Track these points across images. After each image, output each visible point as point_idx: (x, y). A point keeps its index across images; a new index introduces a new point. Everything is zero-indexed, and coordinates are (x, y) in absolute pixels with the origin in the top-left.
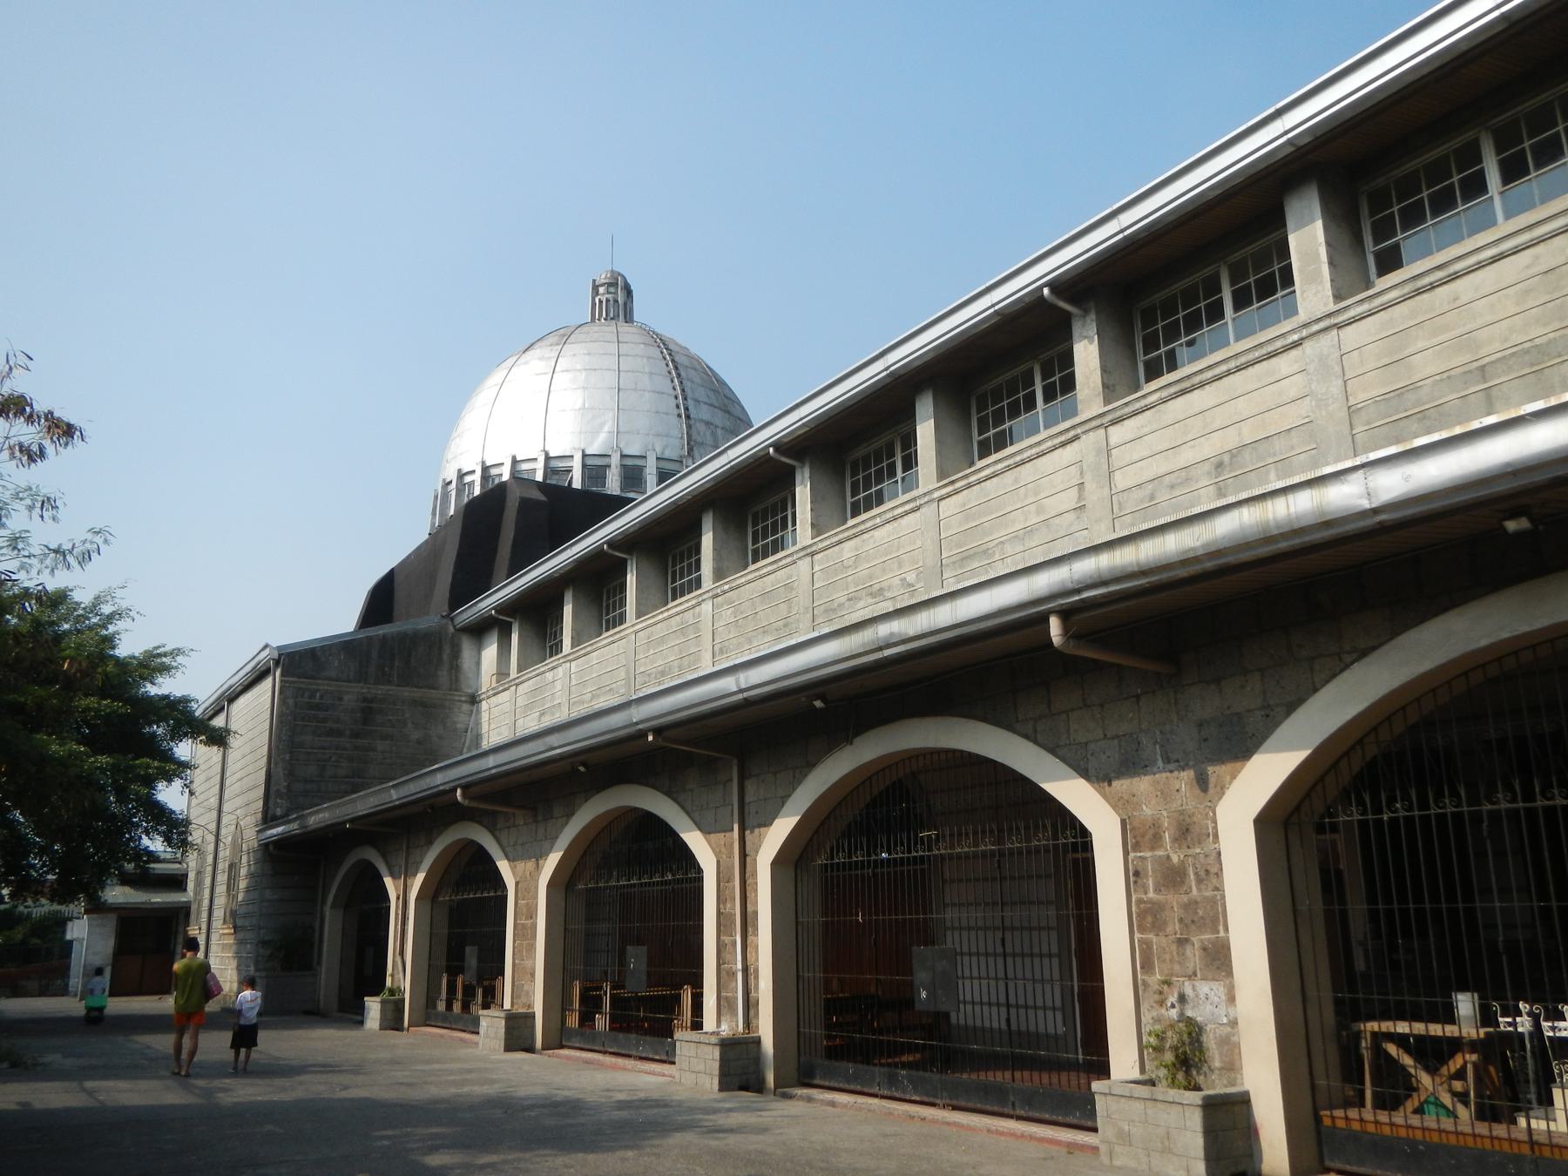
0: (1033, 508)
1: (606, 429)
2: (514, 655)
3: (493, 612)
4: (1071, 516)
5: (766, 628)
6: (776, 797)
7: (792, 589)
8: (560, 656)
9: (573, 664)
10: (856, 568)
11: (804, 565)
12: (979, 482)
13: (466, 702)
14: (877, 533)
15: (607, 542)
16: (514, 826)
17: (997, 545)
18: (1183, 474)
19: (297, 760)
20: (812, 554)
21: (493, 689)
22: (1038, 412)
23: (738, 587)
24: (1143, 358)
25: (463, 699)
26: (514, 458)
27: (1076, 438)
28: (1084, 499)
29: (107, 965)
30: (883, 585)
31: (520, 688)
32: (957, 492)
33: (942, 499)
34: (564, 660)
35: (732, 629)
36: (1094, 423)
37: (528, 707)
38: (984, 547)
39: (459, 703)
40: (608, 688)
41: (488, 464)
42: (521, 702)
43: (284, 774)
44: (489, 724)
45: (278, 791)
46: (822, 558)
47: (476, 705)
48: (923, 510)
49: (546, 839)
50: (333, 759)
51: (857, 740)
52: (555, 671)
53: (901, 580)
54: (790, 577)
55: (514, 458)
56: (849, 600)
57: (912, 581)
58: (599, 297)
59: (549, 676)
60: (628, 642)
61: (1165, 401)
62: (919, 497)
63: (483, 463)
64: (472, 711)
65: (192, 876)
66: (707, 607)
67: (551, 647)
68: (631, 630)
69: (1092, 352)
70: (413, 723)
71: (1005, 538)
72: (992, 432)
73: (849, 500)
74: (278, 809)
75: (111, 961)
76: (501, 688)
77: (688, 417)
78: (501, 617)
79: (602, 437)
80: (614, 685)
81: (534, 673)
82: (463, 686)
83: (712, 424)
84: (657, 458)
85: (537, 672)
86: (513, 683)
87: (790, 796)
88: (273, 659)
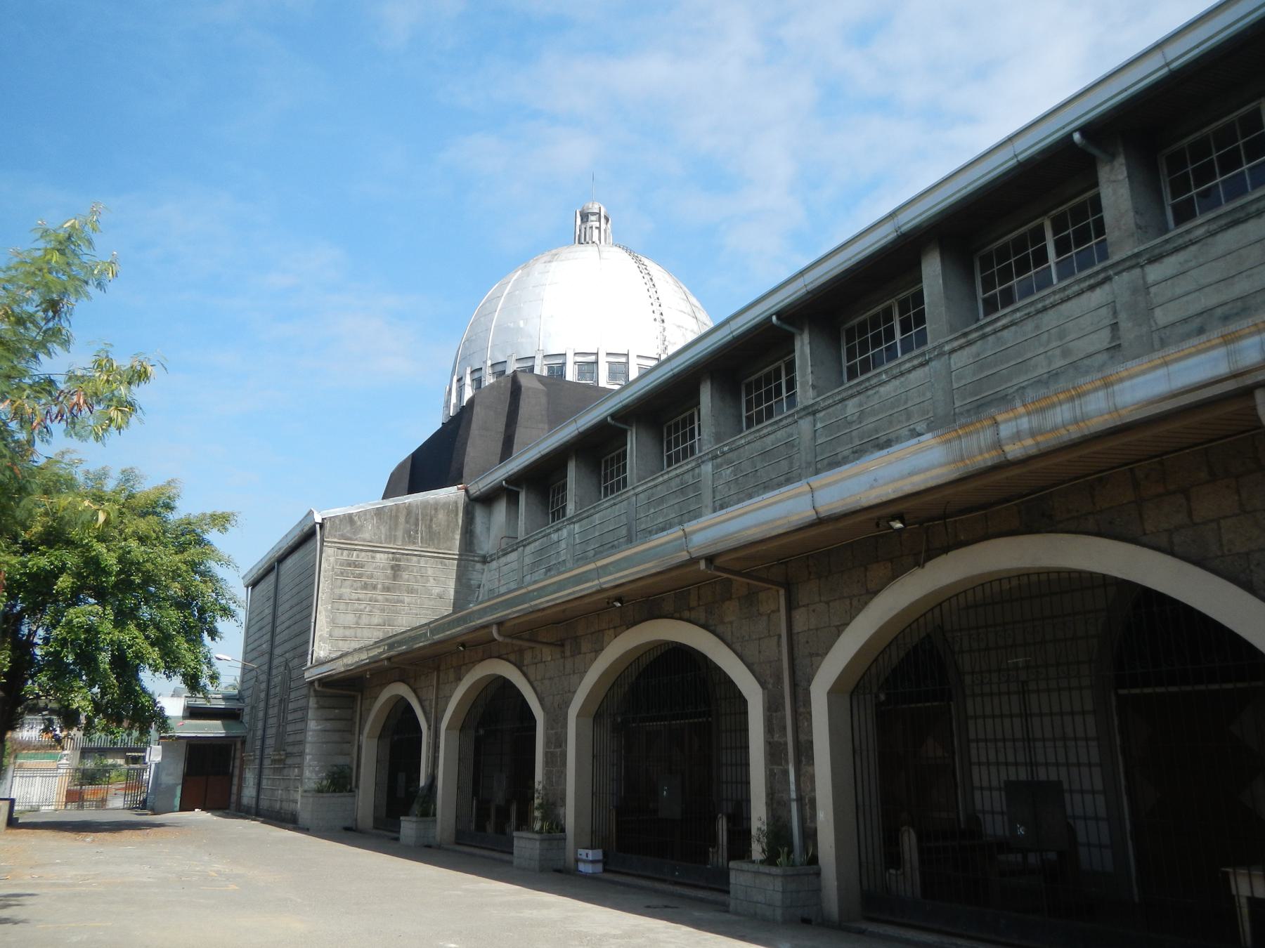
0: (1058, 352)
2: (521, 521)
4: (1105, 356)
5: (766, 484)
6: (830, 626)
7: (793, 446)
8: (565, 519)
9: (577, 526)
10: (860, 422)
11: (805, 425)
12: (995, 332)
13: (478, 562)
14: (882, 389)
16: (542, 662)
17: (1017, 390)
18: (1239, 304)
19: (338, 610)
20: (814, 413)
22: (1050, 266)
23: (739, 448)
24: (1170, 202)
25: (476, 559)
27: (1108, 279)
28: (1119, 338)
29: (177, 785)
30: (890, 436)
32: (970, 344)
33: (953, 351)
35: (732, 486)
36: (1128, 264)
38: (1004, 393)
39: (472, 563)
40: (610, 545)
43: (327, 622)
44: (499, 581)
45: (320, 636)
46: (824, 415)
48: (933, 364)
49: (574, 673)
50: (367, 610)
51: (929, 565)
52: (560, 532)
53: (910, 430)
54: (791, 435)
56: (853, 452)
57: (923, 431)
59: (555, 537)
60: (629, 504)
61: (1213, 234)
62: (929, 352)
64: (484, 570)
65: (247, 710)
66: (707, 468)
67: (553, 514)
68: (632, 492)
69: (1122, 195)
70: (434, 579)
71: (1026, 383)
72: (998, 289)
73: (845, 364)
74: (322, 652)
75: (181, 782)
80: (616, 542)
82: (476, 548)
83: (683, 327)
85: (543, 534)
86: (520, 544)
87: (848, 624)
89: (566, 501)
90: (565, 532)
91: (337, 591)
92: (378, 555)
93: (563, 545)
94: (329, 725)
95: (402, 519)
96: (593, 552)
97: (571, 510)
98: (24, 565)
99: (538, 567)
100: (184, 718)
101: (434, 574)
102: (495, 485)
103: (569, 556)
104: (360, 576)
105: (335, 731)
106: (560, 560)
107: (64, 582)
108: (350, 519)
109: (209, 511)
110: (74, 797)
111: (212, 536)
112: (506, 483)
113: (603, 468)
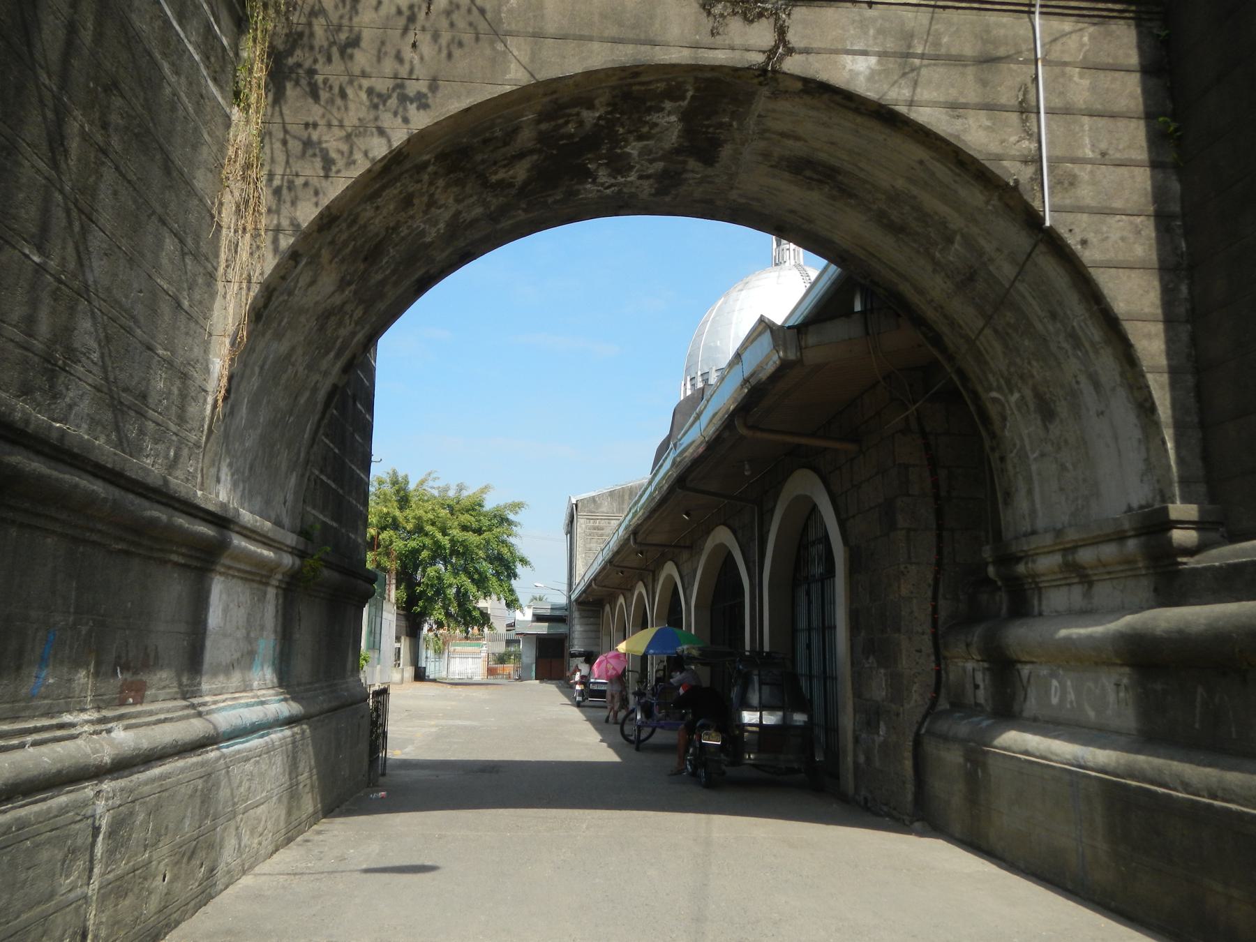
91: (588, 546)
92: (612, 522)
94: (587, 628)
95: (627, 497)
98: (406, 546)
100: (533, 621)
104: (602, 535)
105: (592, 631)
107: (425, 554)
108: (593, 499)
109: (510, 501)
110: (491, 672)
111: (511, 517)
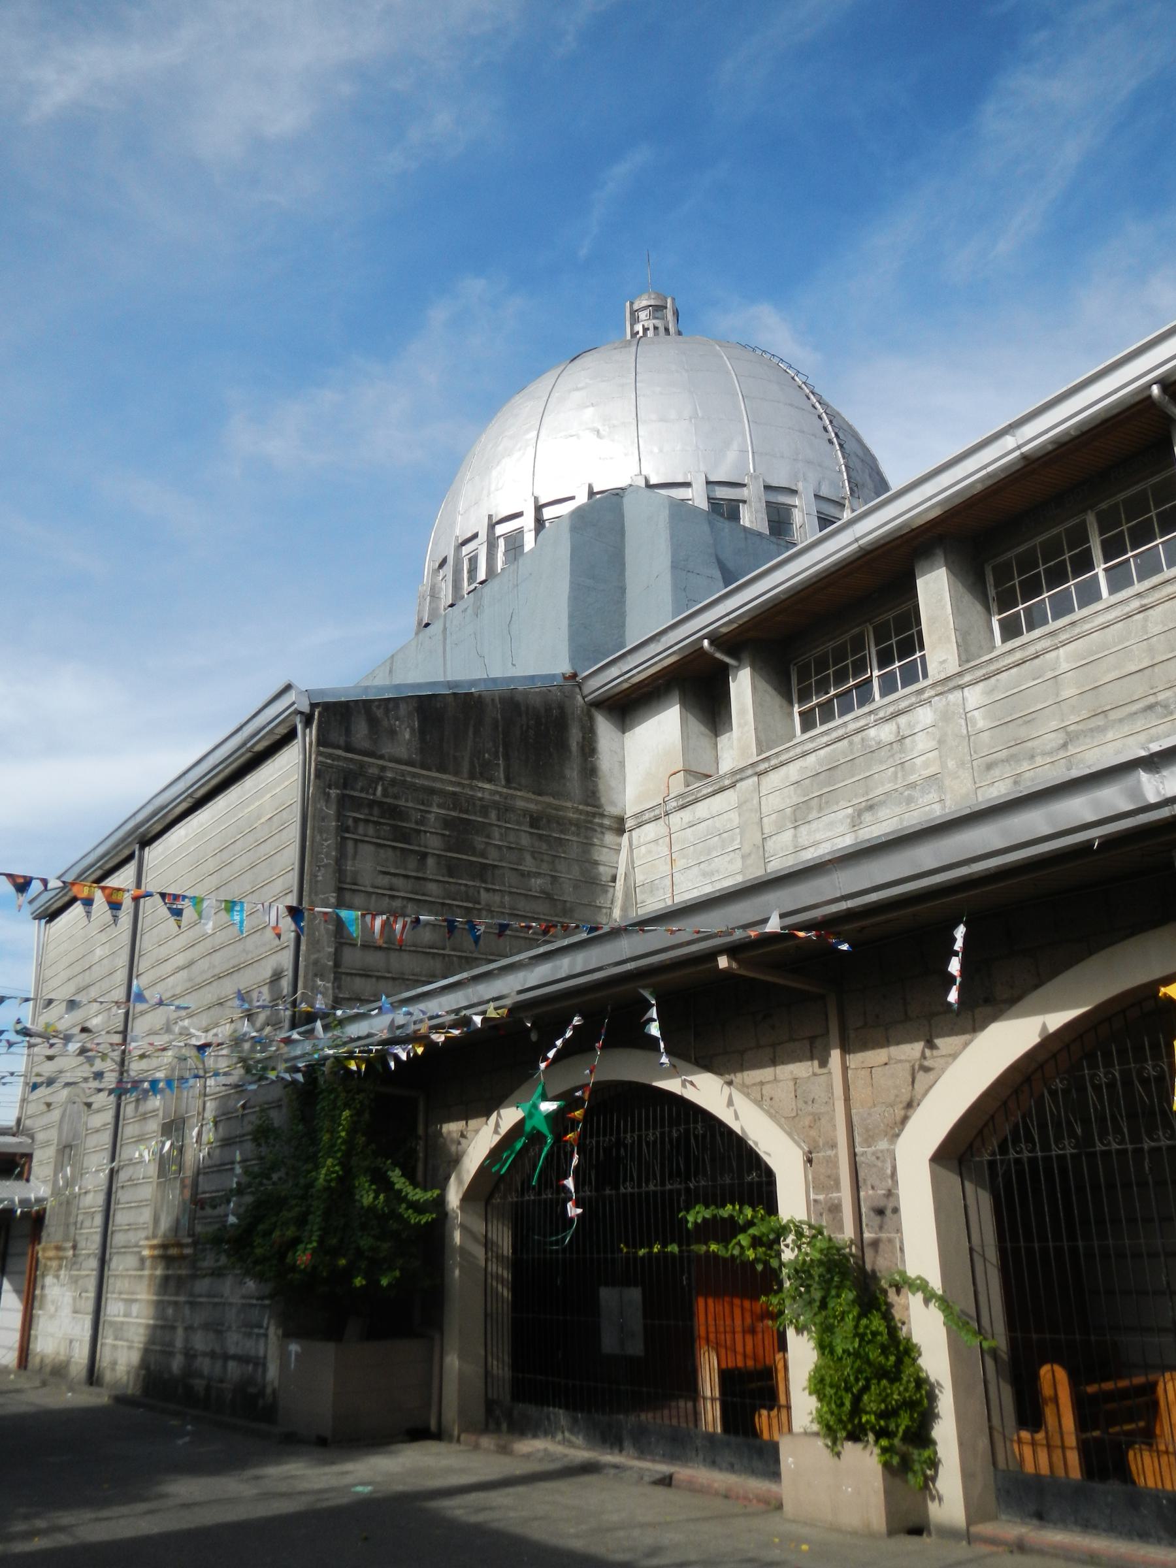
1: (735, 446)
3: (706, 643)
13: (610, 828)
15: (1159, 381)
21: (681, 795)
26: (590, 487)
31: (774, 779)
34: (939, 689)
37: (799, 816)
41: (542, 501)
42: (772, 803)
43: (327, 930)
47: (626, 835)
52: (902, 720)
55: (590, 487)
58: (641, 324)
59: (886, 733)
63: (536, 499)
76: (710, 790)
77: (841, 446)
78: (718, 655)
79: (731, 456)
80: (1168, 693)
81: (825, 739)
84: (817, 496)
86: (750, 772)
88: (301, 713)
89: (922, 648)
90: (925, 716)
93: (922, 743)
96: (1060, 738)
97: (944, 661)
99: (820, 809)
101: (533, 847)
102: (1066, 432)
103: (951, 764)
106: (913, 778)
112: (711, 643)
113: (990, 580)
